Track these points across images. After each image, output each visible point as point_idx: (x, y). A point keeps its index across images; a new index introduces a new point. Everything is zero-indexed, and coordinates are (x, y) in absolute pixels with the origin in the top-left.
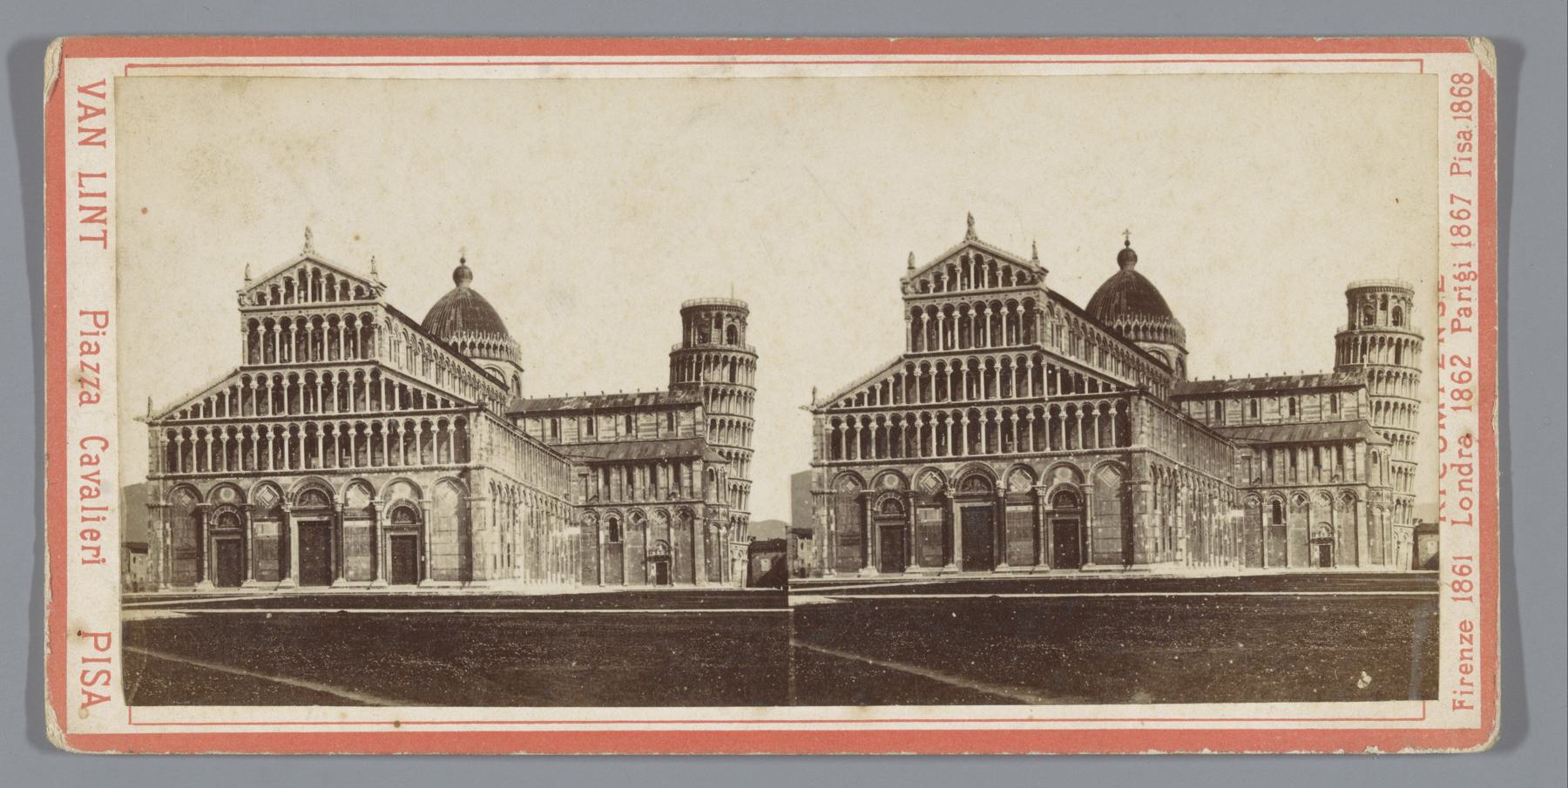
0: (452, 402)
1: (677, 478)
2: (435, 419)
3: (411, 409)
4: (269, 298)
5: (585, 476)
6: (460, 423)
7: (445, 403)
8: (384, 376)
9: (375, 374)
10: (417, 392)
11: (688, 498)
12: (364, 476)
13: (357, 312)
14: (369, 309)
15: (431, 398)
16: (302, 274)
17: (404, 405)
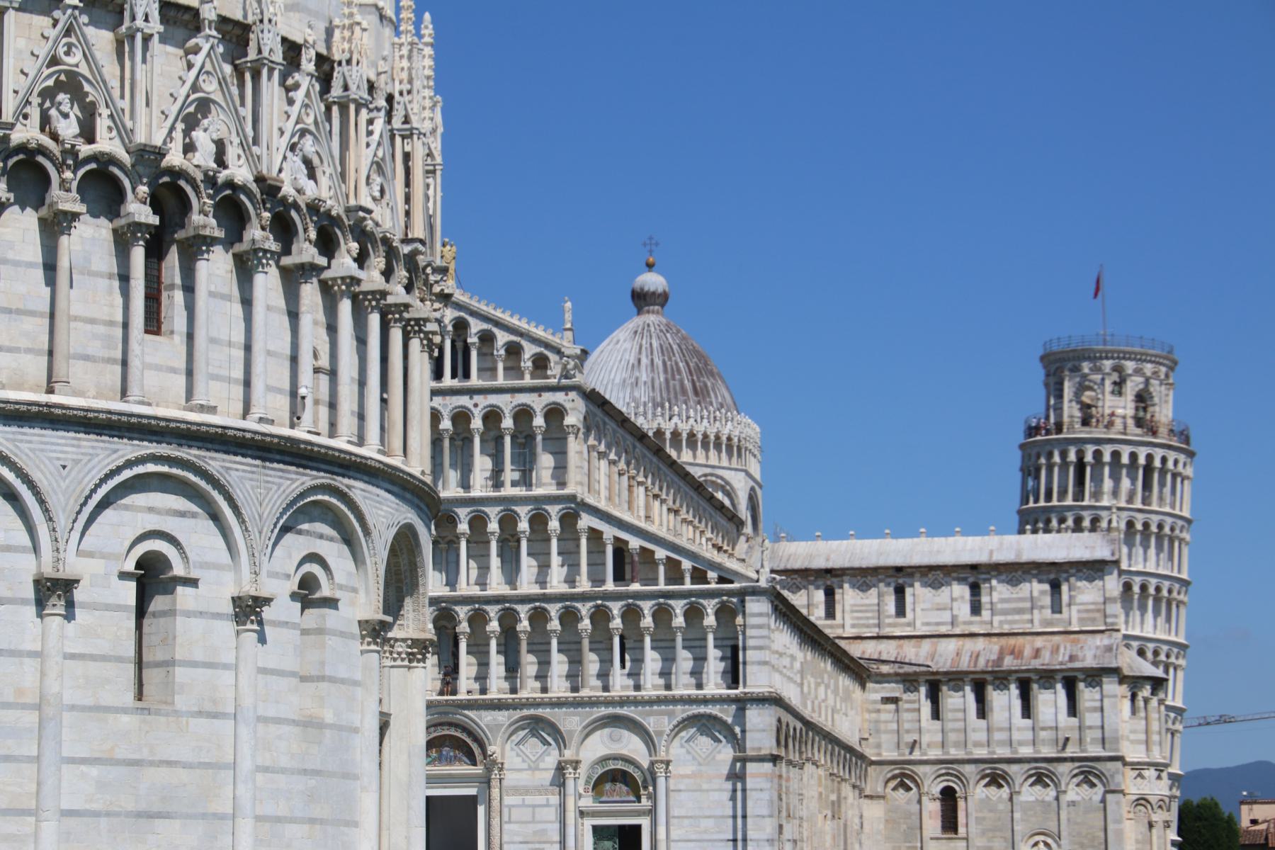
0: (712, 575)
1: (1073, 710)
2: (679, 606)
3: (636, 587)
5: (895, 700)
6: (727, 614)
7: (699, 576)
8: (585, 521)
9: (568, 520)
10: (646, 554)
11: (1094, 750)
12: (540, 712)
13: (538, 403)
14: (559, 397)
15: (673, 566)
17: (619, 577)
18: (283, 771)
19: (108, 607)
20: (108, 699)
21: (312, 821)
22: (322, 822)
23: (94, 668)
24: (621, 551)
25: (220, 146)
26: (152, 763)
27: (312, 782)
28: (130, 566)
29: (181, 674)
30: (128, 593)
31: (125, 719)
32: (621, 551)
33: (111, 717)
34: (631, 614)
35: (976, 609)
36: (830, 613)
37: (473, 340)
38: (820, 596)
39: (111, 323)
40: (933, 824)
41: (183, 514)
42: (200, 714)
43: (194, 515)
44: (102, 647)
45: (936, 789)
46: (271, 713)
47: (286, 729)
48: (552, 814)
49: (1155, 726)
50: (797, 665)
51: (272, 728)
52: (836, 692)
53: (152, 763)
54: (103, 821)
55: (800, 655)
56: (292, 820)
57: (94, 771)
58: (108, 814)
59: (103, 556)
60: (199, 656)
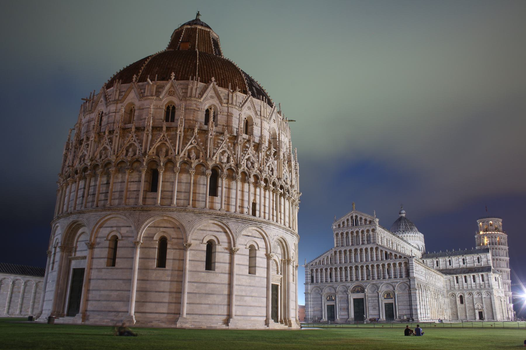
0: (403, 257)
4: (342, 226)
8: (380, 248)
10: (391, 254)
15: (396, 255)
16: (352, 217)
17: (386, 258)
18: (244, 286)
19: (200, 250)
20: (199, 269)
21: (252, 296)
22: (255, 297)
23: (196, 263)
24: (386, 253)
25: (228, 158)
26: (209, 283)
27: (252, 288)
28: (205, 241)
29: (217, 265)
30: (204, 247)
31: (203, 274)
32: (386, 253)
33: (200, 273)
34: (389, 265)
35: (464, 263)
36: (437, 266)
37: (359, 219)
38: (435, 263)
39: (204, 194)
40: (458, 302)
41: (218, 232)
42: (222, 273)
43: (221, 232)
44: (198, 259)
45: (459, 295)
46: (241, 273)
47: (245, 277)
48: (377, 301)
49: (500, 283)
50: (423, 273)
51: (241, 276)
52: (435, 278)
53: (209, 283)
54: (198, 295)
55: (425, 272)
56: (246, 296)
57: (195, 284)
58: (198, 293)
59: (199, 240)
60: (221, 261)
